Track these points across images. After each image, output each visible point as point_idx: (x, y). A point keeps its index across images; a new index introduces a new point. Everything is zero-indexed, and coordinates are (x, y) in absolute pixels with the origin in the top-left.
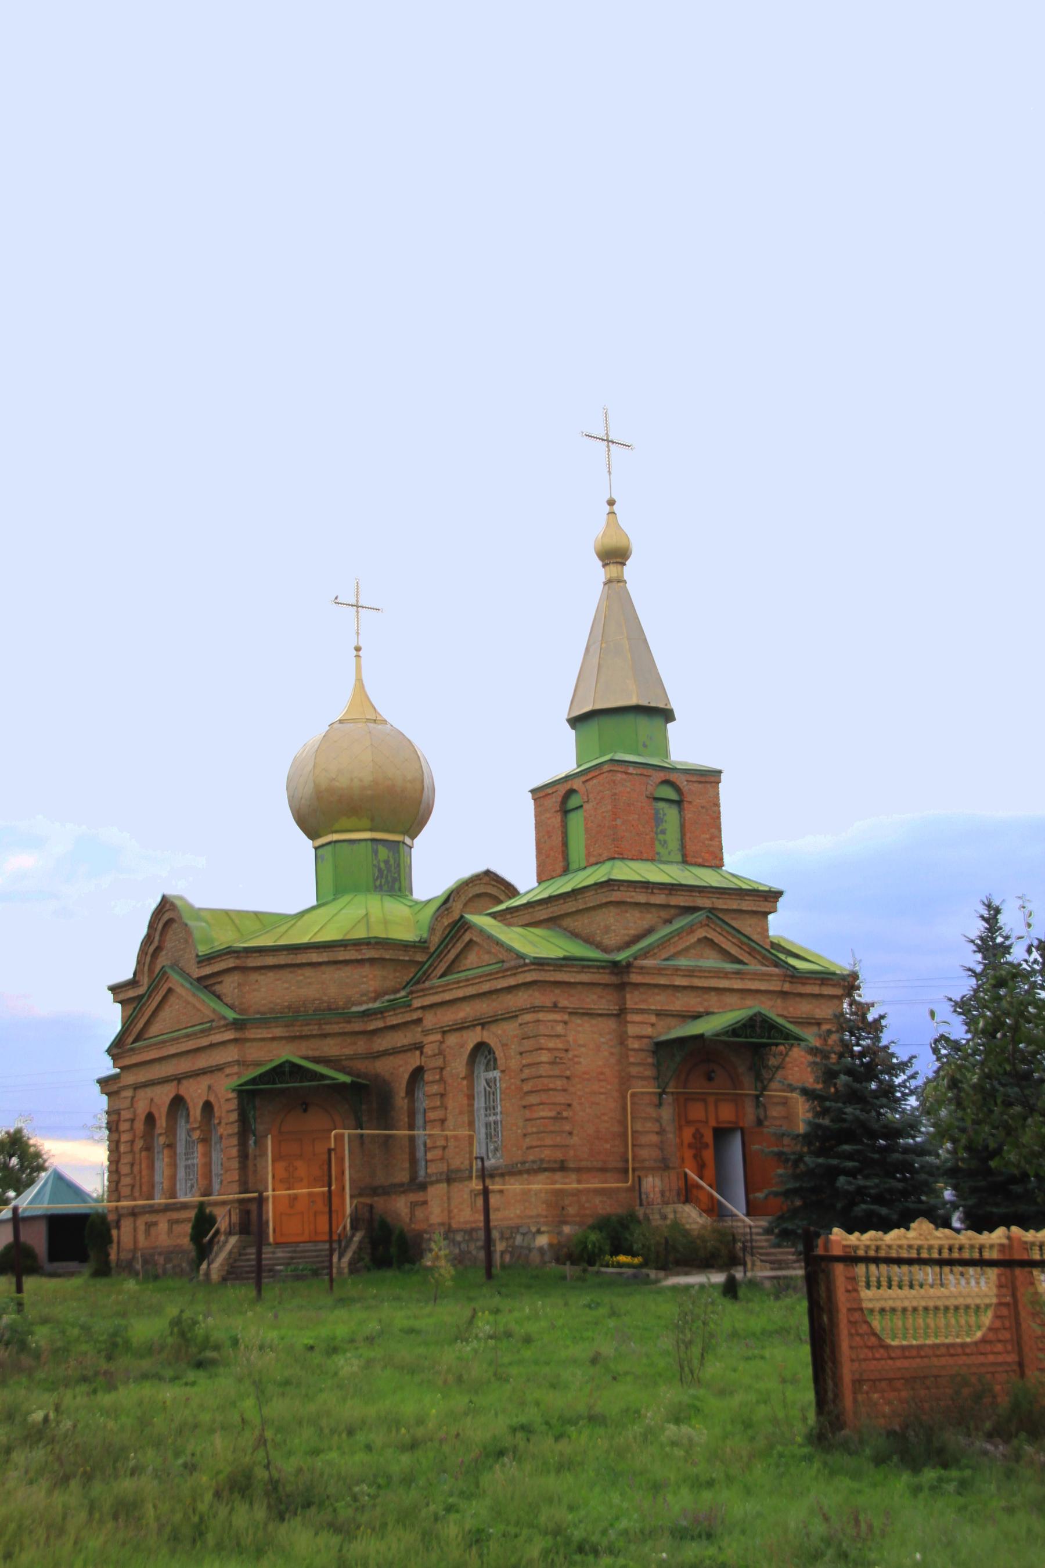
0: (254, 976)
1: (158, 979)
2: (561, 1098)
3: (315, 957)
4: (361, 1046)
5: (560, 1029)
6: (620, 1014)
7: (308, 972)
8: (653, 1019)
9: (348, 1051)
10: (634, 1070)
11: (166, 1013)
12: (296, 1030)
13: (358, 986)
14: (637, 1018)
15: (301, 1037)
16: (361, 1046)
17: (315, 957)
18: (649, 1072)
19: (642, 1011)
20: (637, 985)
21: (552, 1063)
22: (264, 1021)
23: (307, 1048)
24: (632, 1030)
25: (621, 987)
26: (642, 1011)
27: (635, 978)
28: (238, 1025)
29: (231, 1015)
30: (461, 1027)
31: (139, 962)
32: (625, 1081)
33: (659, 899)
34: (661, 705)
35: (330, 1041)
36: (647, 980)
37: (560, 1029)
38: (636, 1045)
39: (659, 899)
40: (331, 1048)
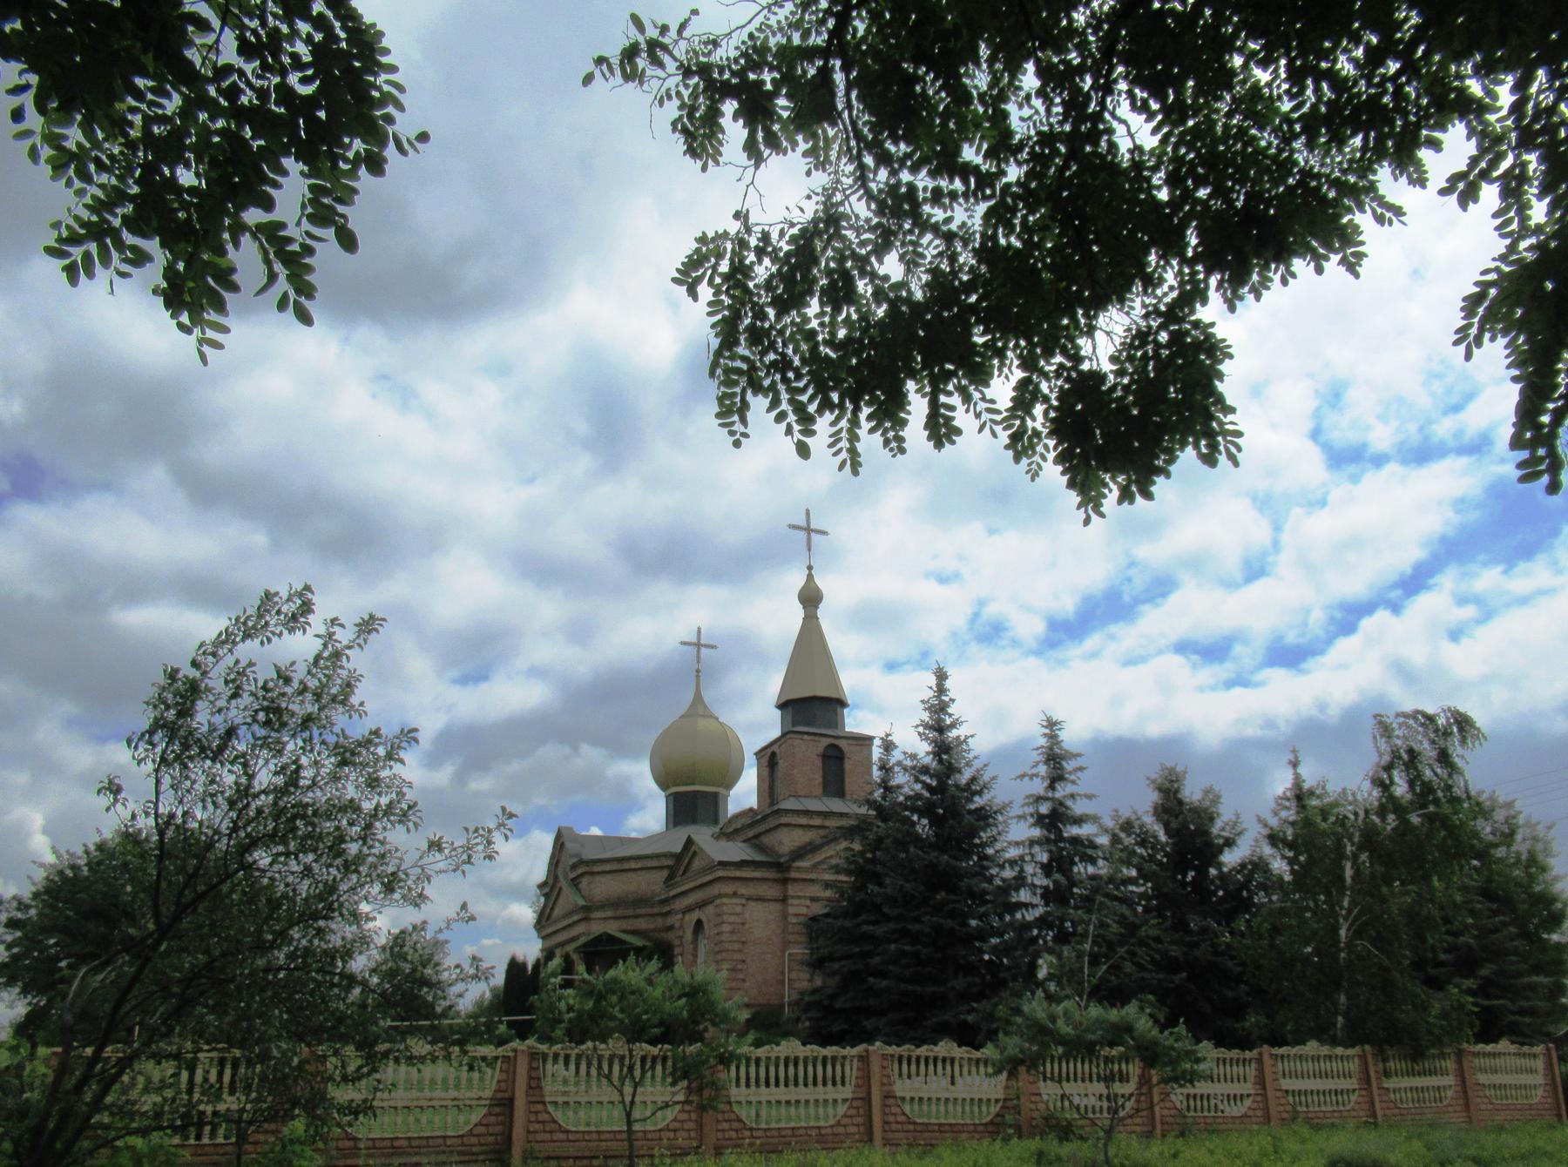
0: (598, 878)
1: (556, 878)
2: (737, 956)
3: (633, 865)
4: (659, 922)
5: (738, 909)
6: (784, 900)
7: (630, 874)
8: (808, 902)
9: (652, 926)
10: (791, 938)
11: (561, 901)
12: (620, 912)
13: (650, 883)
14: (796, 902)
15: (625, 917)
16: (659, 922)
17: (633, 865)
18: (803, 939)
19: (799, 897)
20: (795, 880)
21: (732, 932)
22: (602, 906)
23: (624, 924)
24: (791, 910)
25: (785, 881)
26: (799, 897)
27: (793, 875)
28: (586, 909)
29: (581, 902)
30: (690, 909)
31: (549, 871)
32: (786, 944)
33: (817, 821)
34: (834, 695)
35: (641, 920)
36: (804, 876)
37: (738, 909)
38: (794, 920)
39: (817, 821)
40: (641, 924)
